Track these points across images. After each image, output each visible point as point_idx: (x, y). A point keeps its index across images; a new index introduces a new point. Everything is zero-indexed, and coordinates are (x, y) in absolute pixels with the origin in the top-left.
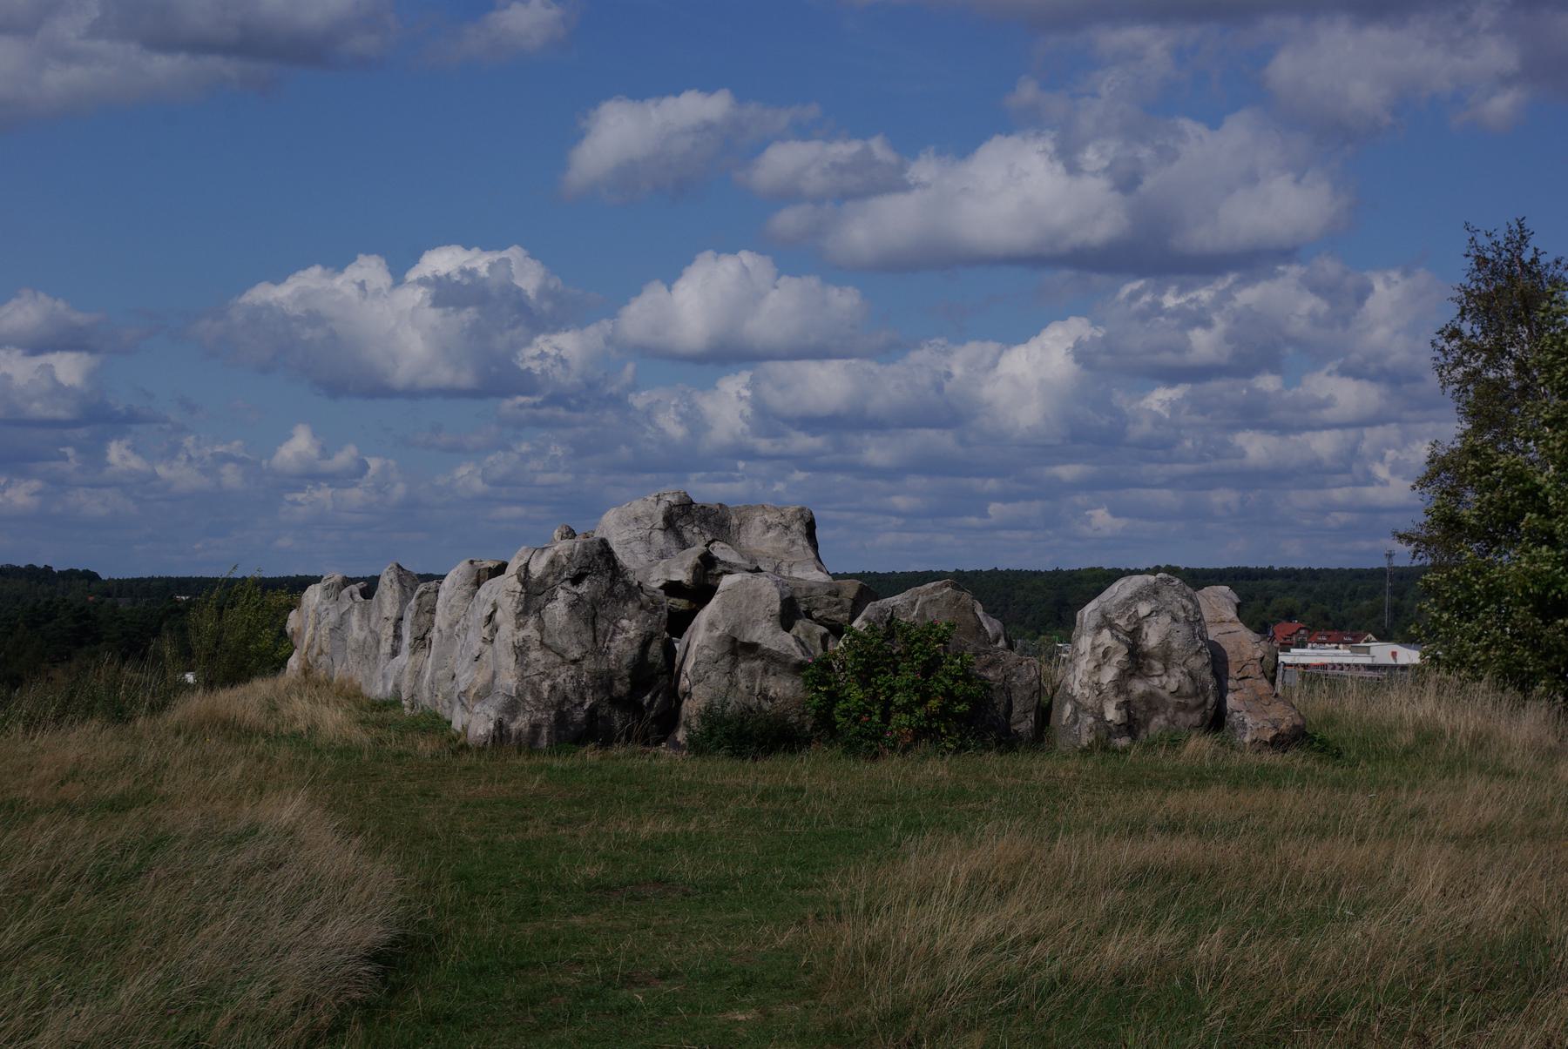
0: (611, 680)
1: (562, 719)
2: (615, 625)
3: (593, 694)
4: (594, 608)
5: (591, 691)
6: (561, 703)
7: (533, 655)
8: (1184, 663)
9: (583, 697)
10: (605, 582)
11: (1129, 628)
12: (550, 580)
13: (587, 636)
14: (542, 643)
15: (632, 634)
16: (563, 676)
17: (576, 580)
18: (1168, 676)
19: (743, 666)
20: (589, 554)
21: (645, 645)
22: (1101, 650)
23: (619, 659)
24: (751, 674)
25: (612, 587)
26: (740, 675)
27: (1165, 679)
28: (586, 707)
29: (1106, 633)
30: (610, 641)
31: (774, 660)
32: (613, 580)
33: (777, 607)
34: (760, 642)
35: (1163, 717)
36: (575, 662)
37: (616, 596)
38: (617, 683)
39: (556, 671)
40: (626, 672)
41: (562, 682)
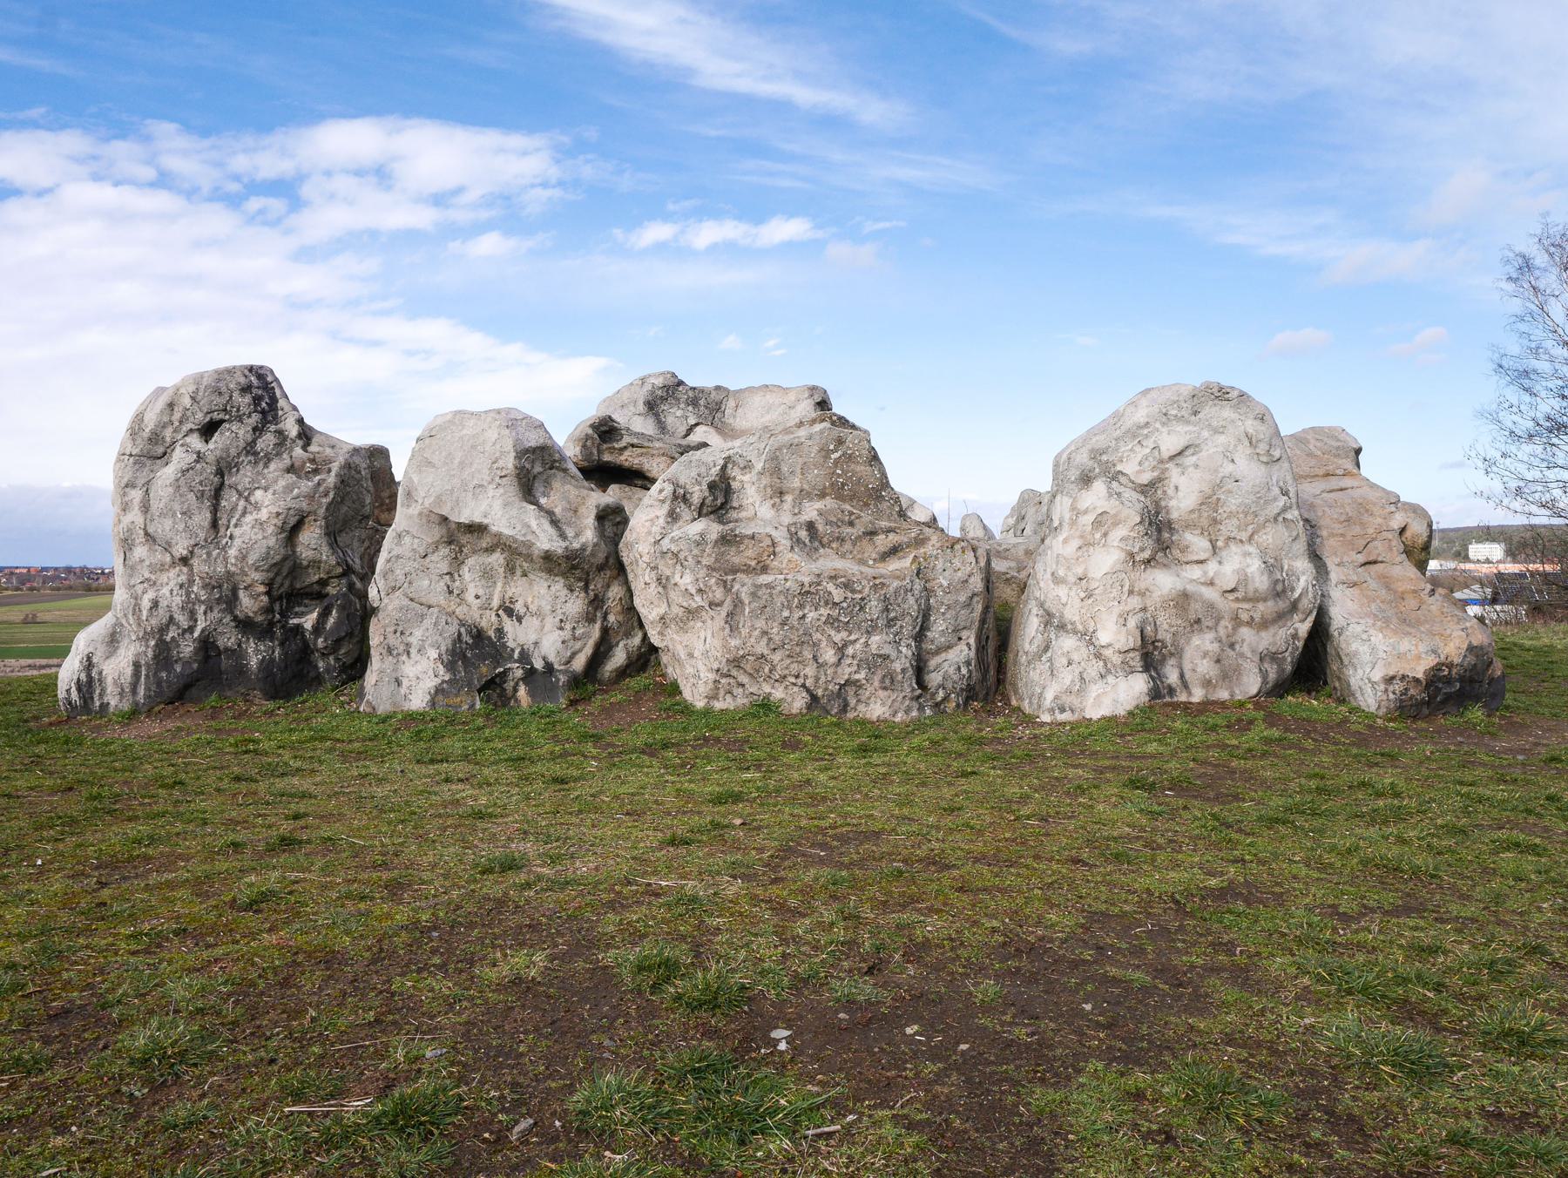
0: (234, 590)
1: (163, 654)
2: (247, 499)
3: (205, 613)
4: (220, 473)
5: (203, 608)
6: (163, 630)
7: (140, 551)
8: (1251, 538)
9: (192, 616)
10: (242, 431)
11: (1145, 478)
12: (168, 434)
13: (202, 518)
14: (147, 534)
15: (264, 514)
16: (172, 584)
17: (209, 430)
18: (1220, 563)
19: (471, 561)
20: (224, 389)
21: (291, 531)
22: (1090, 518)
23: (243, 557)
24: (487, 574)
25: (254, 442)
26: (467, 576)
27: (1212, 567)
28: (196, 635)
29: (1099, 486)
30: (236, 526)
31: (516, 555)
32: (258, 430)
33: (509, 462)
34: (486, 521)
35: (1210, 636)
36: (184, 561)
37: (256, 454)
38: (241, 594)
39: (164, 578)
40: (257, 576)
41: (168, 594)
